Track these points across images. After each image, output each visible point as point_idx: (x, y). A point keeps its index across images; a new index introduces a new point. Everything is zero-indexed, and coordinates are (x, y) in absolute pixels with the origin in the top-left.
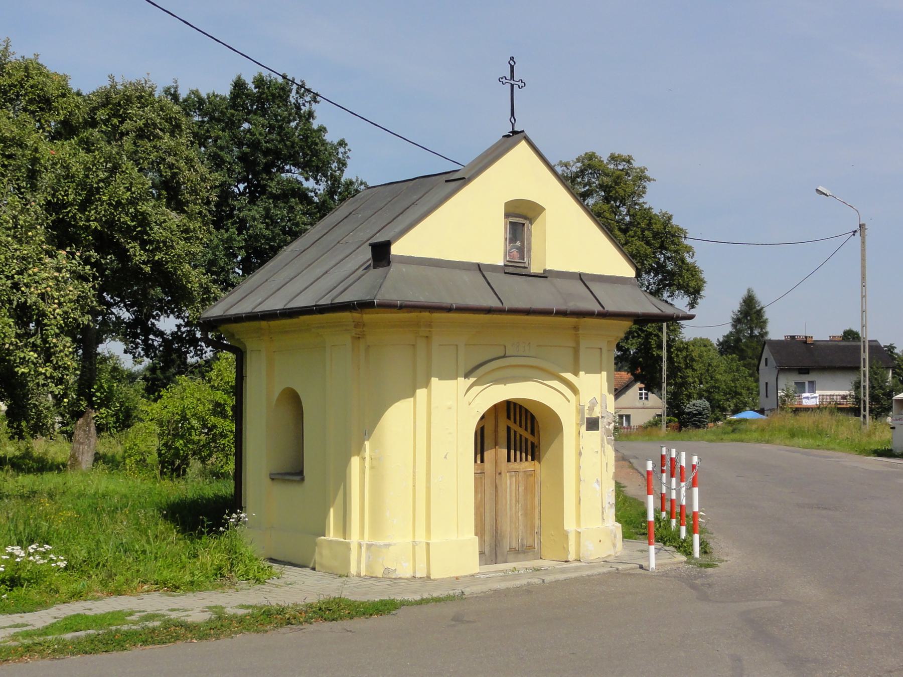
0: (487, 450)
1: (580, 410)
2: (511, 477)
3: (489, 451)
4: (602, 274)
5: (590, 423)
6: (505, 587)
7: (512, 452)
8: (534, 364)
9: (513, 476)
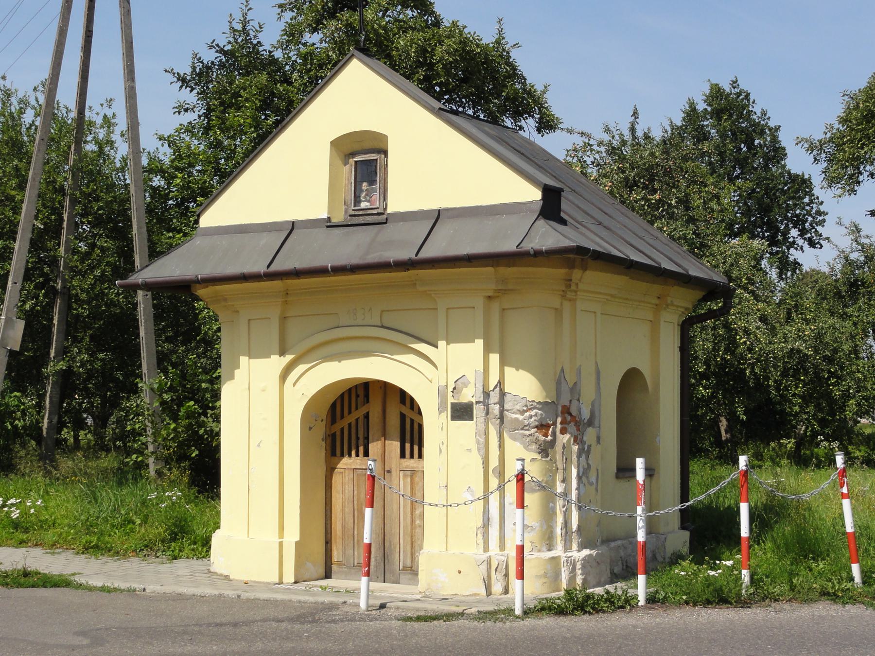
0: (373, 442)
1: (442, 393)
2: (405, 476)
3: (375, 444)
4: (479, 204)
5: (457, 410)
6: (191, 593)
7: (408, 446)
8: (366, 334)
9: (407, 475)
